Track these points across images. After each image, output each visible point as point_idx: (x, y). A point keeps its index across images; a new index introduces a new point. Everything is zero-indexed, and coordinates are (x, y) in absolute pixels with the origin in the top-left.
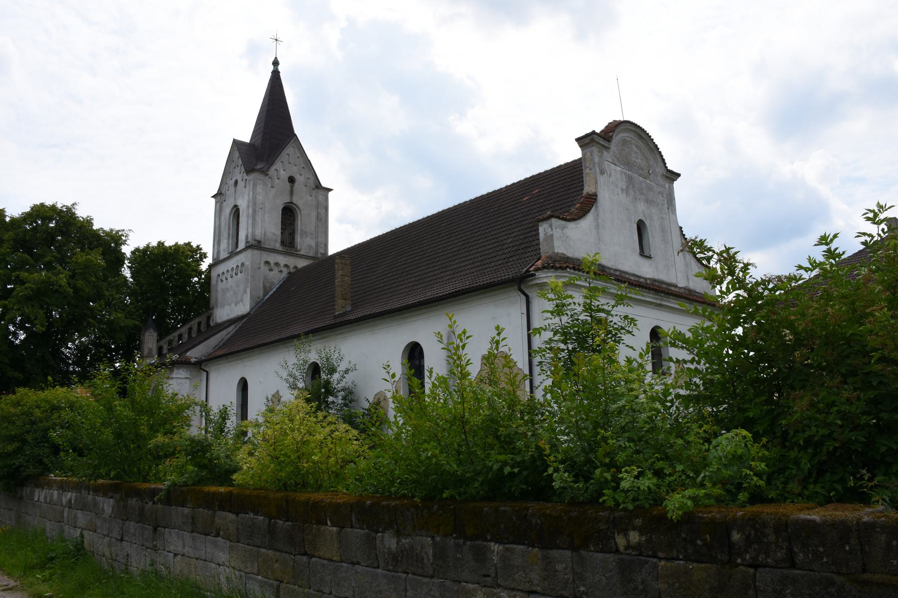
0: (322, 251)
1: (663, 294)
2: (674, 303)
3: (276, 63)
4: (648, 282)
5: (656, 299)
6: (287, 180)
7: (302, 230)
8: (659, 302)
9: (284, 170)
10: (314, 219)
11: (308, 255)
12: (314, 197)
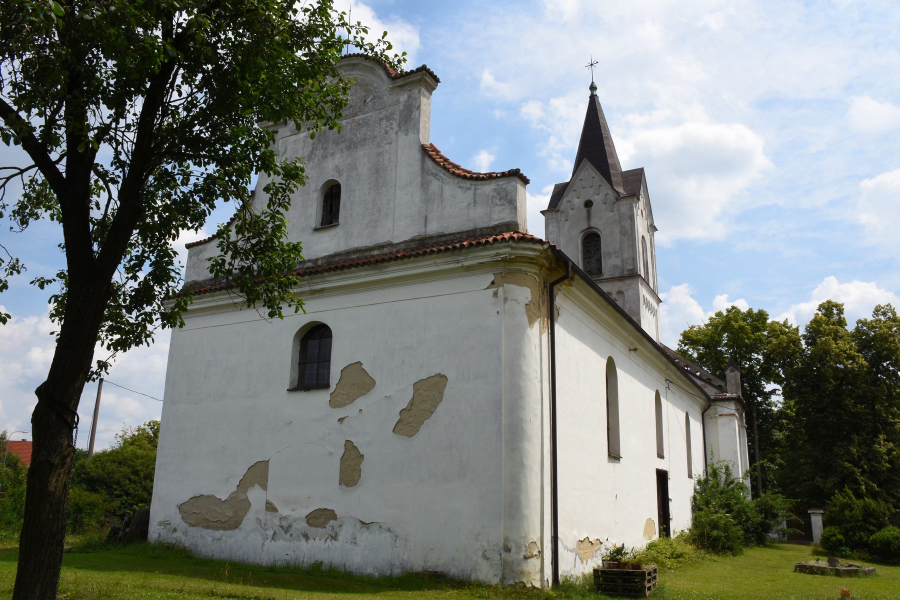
0: (630, 267)
2: (394, 271)
3: (593, 88)
4: (320, 263)
6: (583, 206)
7: (604, 252)
8: (307, 289)
11: (613, 276)
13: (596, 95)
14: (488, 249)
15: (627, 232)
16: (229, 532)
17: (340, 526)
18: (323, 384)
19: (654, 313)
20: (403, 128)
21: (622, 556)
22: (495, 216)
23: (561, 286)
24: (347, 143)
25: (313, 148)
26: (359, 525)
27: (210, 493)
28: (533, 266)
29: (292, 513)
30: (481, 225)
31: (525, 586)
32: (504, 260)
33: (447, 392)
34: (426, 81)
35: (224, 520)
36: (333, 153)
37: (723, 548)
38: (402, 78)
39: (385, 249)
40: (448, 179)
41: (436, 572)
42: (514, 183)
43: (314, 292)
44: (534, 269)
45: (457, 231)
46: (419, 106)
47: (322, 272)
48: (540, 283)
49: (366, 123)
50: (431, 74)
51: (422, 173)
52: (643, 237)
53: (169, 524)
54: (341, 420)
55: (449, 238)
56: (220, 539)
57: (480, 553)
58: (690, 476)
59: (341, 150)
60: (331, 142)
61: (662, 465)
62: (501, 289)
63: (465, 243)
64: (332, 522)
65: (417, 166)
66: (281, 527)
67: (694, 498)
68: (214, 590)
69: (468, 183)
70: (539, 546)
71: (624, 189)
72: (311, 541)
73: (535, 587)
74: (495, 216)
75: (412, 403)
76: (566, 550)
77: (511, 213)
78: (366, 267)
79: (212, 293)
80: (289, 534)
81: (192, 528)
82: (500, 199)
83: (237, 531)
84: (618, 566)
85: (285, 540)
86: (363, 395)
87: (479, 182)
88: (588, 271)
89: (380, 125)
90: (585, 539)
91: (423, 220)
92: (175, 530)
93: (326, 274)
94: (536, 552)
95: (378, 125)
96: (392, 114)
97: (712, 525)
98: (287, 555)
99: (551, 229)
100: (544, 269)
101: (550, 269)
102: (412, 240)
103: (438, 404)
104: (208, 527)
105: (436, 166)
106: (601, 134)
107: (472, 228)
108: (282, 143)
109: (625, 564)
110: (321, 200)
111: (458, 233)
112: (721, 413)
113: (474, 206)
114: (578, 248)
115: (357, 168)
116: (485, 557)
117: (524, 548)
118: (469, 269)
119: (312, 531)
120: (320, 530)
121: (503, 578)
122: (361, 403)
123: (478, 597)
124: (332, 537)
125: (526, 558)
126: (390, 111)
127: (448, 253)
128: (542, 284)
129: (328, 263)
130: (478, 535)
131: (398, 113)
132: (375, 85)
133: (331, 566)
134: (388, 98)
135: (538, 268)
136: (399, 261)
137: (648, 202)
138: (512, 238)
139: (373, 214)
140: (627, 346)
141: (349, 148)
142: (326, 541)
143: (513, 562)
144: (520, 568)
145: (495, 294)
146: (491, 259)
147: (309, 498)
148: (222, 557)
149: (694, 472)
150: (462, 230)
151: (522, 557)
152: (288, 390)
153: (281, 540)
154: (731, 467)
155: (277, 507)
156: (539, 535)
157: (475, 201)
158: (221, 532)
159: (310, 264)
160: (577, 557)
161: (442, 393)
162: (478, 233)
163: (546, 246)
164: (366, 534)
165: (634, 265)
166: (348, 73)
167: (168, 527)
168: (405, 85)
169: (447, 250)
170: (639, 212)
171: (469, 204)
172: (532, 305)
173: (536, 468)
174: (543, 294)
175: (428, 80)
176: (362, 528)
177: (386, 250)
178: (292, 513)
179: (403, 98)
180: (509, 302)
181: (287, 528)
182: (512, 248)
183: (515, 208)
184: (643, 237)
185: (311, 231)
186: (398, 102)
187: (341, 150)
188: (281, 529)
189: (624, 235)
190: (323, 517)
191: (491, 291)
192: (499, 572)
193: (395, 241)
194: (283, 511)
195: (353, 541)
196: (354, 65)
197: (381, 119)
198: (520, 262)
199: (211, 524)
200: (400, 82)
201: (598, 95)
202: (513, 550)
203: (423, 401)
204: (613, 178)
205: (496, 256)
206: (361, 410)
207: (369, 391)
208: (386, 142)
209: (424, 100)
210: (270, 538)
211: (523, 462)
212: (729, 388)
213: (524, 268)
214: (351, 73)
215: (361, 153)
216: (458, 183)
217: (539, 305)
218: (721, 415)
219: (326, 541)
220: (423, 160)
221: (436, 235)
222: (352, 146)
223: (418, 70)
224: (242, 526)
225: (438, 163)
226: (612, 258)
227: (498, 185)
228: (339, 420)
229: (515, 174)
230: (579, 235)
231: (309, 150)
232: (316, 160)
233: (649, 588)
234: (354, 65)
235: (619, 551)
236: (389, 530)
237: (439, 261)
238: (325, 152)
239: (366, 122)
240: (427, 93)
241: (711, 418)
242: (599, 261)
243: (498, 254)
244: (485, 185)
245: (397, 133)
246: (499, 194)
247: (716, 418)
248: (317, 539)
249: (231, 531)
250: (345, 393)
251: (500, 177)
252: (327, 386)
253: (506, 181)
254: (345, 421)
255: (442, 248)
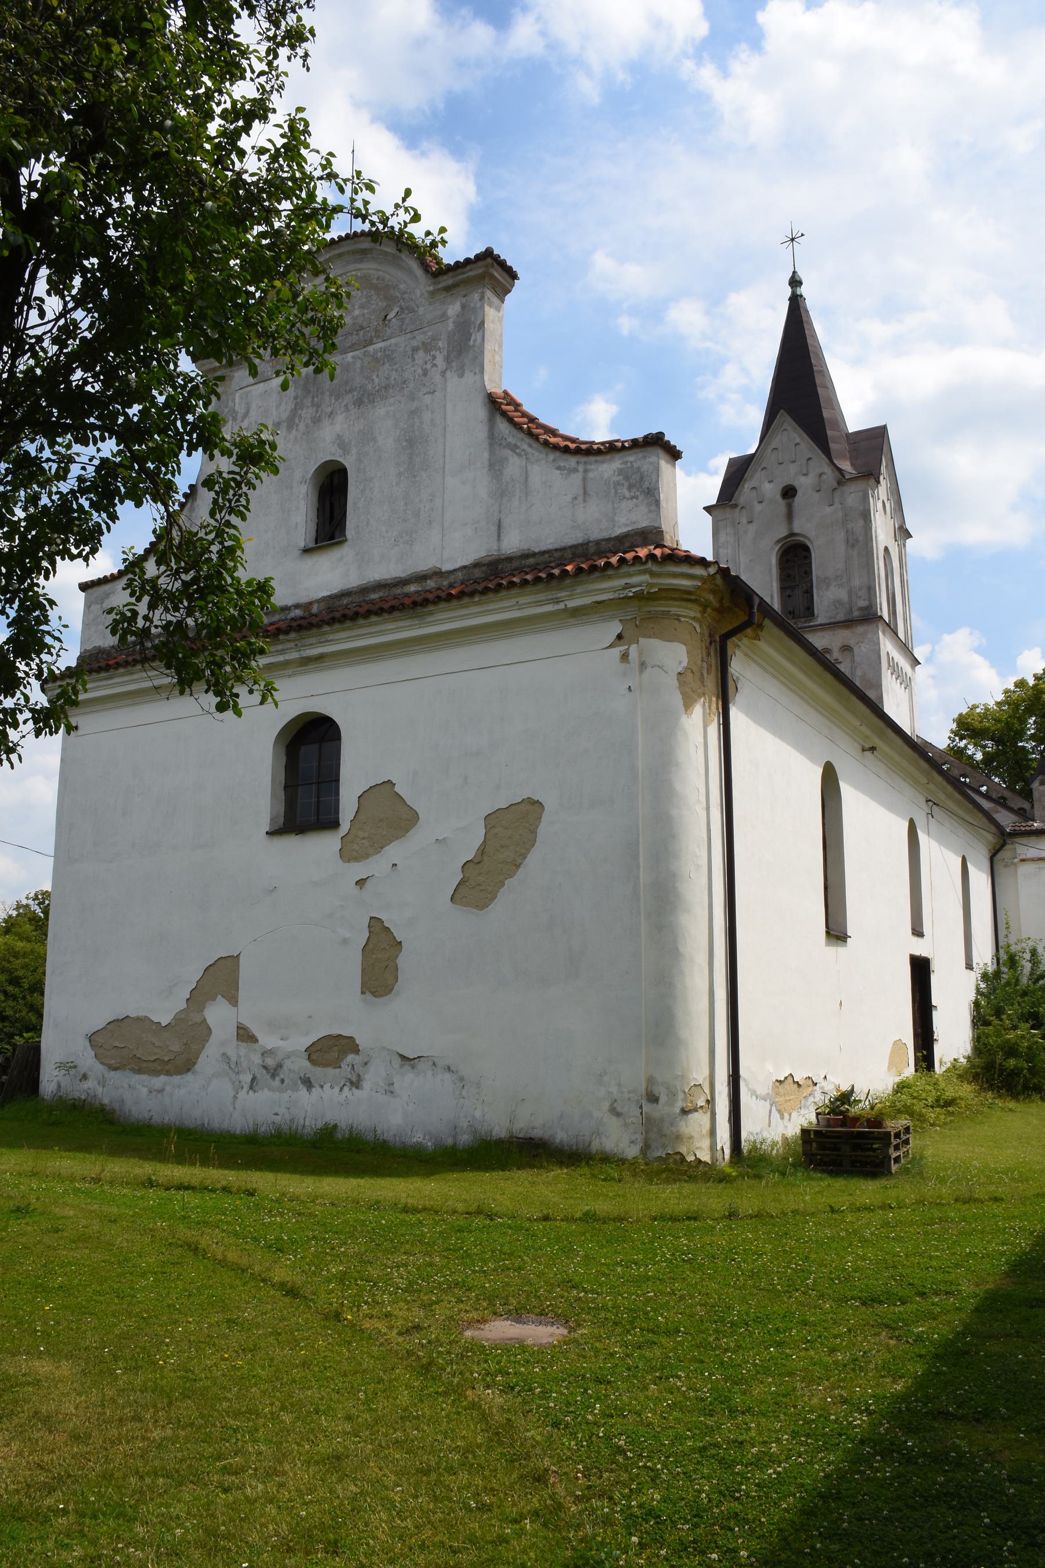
0: (862, 603)
1: (293, 635)
3: (795, 282)
4: (315, 609)
5: (282, 652)
6: (779, 497)
7: (817, 578)
8: (294, 655)
9: (770, 482)
10: (841, 548)
11: (833, 620)
12: (837, 505)
13: (801, 296)
14: (610, 577)
15: (857, 541)
16: (176, 1079)
17: (366, 1064)
18: (328, 822)
19: (907, 683)
20: (454, 364)
21: (850, 1105)
22: (622, 519)
23: (740, 640)
24: (355, 393)
25: (296, 405)
26: (397, 1061)
27: (141, 1014)
28: (690, 605)
29: (281, 1043)
30: (596, 534)
31: (683, 1159)
32: (639, 597)
33: (543, 829)
34: (492, 277)
35: (166, 1059)
36: (332, 413)
37: (1026, 1088)
38: (450, 274)
39: (428, 581)
40: (536, 454)
41: (531, 1138)
42: (653, 459)
43: (306, 662)
44: (692, 611)
45: (556, 546)
46: (483, 323)
47: (318, 626)
48: (702, 634)
49: (388, 356)
50: (502, 265)
51: (491, 445)
52: (886, 549)
53: (75, 1067)
54: (361, 883)
55: (541, 559)
56: (161, 1091)
57: (606, 1105)
58: (969, 966)
59: (346, 406)
60: (328, 393)
61: (921, 948)
62: (633, 649)
63: (569, 568)
64: (351, 1058)
65: (481, 432)
66: (265, 1067)
67: (976, 1004)
68: (154, 1178)
69: (572, 461)
70: (707, 1091)
71: (852, 464)
72: (316, 1091)
73: (700, 1161)
74: (622, 519)
75: (482, 851)
76: (754, 1097)
77: (650, 511)
78: (396, 614)
79: (130, 668)
80: (277, 1079)
81: (113, 1073)
82: (630, 487)
83: (189, 1077)
84: (843, 1123)
85: (271, 1089)
86: (397, 838)
87: (592, 459)
88: (790, 612)
89: (414, 360)
90: (786, 1078)
91: (494, 528)
92: (85, 1077)
93: (326, 628)
94: (701, 1102)
95: (410, 360)
96: (435, 339)
97: (1006, 1049)
98: (276, 1114)
99: (723, 538)
100: (709, 610)
101: (721, 611)
102: (476, 565)
103: (528, 850)
104: (140, 1071)
105: (514, 431)
106: (811, 365)
107: (580, 541)
108: (241, 398)
109: (856, 1119)
110: (313, 498)
111: (556, 550)
112: (1024, 857)
113: (584, 501)
114: (771, 570)
115: (374, 440)
116: (615, 1112)
117: (681, 1096)
118: (577, 613)
119: (317, 1073)
120: (330, 1071)
121: (646, 1147)
122: (395, 852)
123: (603, 1180)
124: (352, 1083)
125: (685, 1112)
126: (430, 333)
127: (540, 586)
128: (706, 637)
129: (330, 610)
130: (601, 1075)
131: (444, 337)
132: (402, 286)
133: (351, 1131)
134: (426, 311)
135: (700, 609)
136: (455, 603)
137: (894, 486)
138: (651, 557)
139: (405, 521)
140: (859, 743)
141: (359, 403)
142: (341, 1090)
143: (662, 1120)
144: (674, 1129)
145: (625, 657)
146: (616, 595)
147: (310, 1017)
148: (166, 1121)
149: (976, 959)
150: (563, 545)
151: (678, 1111)
152: (267, 833)
153: (266, 1090)
154: (1040, 950)
155: (256, 1034)
156: (706, 1072)
157: (585, 493)
158: (163, 1078)
159: (298, 612)
160: (774, 1108)
161: (534, 832)
162: (592, 550)
163: (712, 570)
164: (410, 1076)
165: (870, 599)
166: (352, 267)
167: (73, 1072)
168: (455, 285)
169: (538, 580)
170: (880, 505)
171: (575, 498)
172: (690, 675)
173: (702, 958)
174: (708, 655)
175: (496, 274)
176: (402, 1066)
177: (431, 584)
178: (281, 1043)
179: (453, 309)
180: (649, 670)
181: (275, 1070)
182: (652, 574)
183: (657, 503)
184: (886, 549)
185: (298, 553)
186: (444, 317)
187: (346, 406)
188: (264, 1071)
189: (853, 546)
190: (335, 1049)
191: (617, 651)
192: (640, 1138)
193: (447, 567)
194: (267, 1040)
195: (387, 1088)
196: (364, 252)
197: (415, 350)
198: (666, 599)
199: (144, 1065)
200: (447, 280)
201: (804, 295)
202: (663, 1099)
203: (502, 847)
204: (833, 446)
205: (624, 589)
206: (395, 865)
207: (407, 831)
208: (425, 390)
209: (490, 313)
210: (246, 1087)
211: (677, 949)
212: (1037, 813)
213: (674, 610)
214: (359, 266)
215: (380, 411)
216: (554, 461)
217: (702, 675)
218: (1023, 860)
219: (341, 1090)
220: (491, 421)
221: (519, 554)
222: (364, 399)
223: (479, 257)
224: (197, 1067)
225: (518, 426)
226: (832, 588)
227: (626, 463)
228: (357, 883)
229: (656, 442)
230: (772, 548)
231: (289, 408)
232: (302, 427)
233: (897, 1160)
234: (364, 252)
235: (846, 1097)
236: (449, 1068)
237: (522, 600)
238: (317, 411)
239: (387, 356)
240: (495, 300)
241: (1006, 866)
242: (809, 592)
243: (628, 586)
244: (603, 462)
245: (443, 373)
246: (627, 478)
247: (1015, 864)
248: (327, 1086)
249: (179, 1077)
250: (366, 835)
251: (630, 448)
252: (334, 825)
253: (640, 455)
254: (368, 883)
255: (529, 577)
